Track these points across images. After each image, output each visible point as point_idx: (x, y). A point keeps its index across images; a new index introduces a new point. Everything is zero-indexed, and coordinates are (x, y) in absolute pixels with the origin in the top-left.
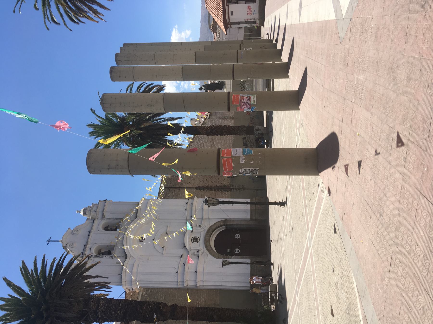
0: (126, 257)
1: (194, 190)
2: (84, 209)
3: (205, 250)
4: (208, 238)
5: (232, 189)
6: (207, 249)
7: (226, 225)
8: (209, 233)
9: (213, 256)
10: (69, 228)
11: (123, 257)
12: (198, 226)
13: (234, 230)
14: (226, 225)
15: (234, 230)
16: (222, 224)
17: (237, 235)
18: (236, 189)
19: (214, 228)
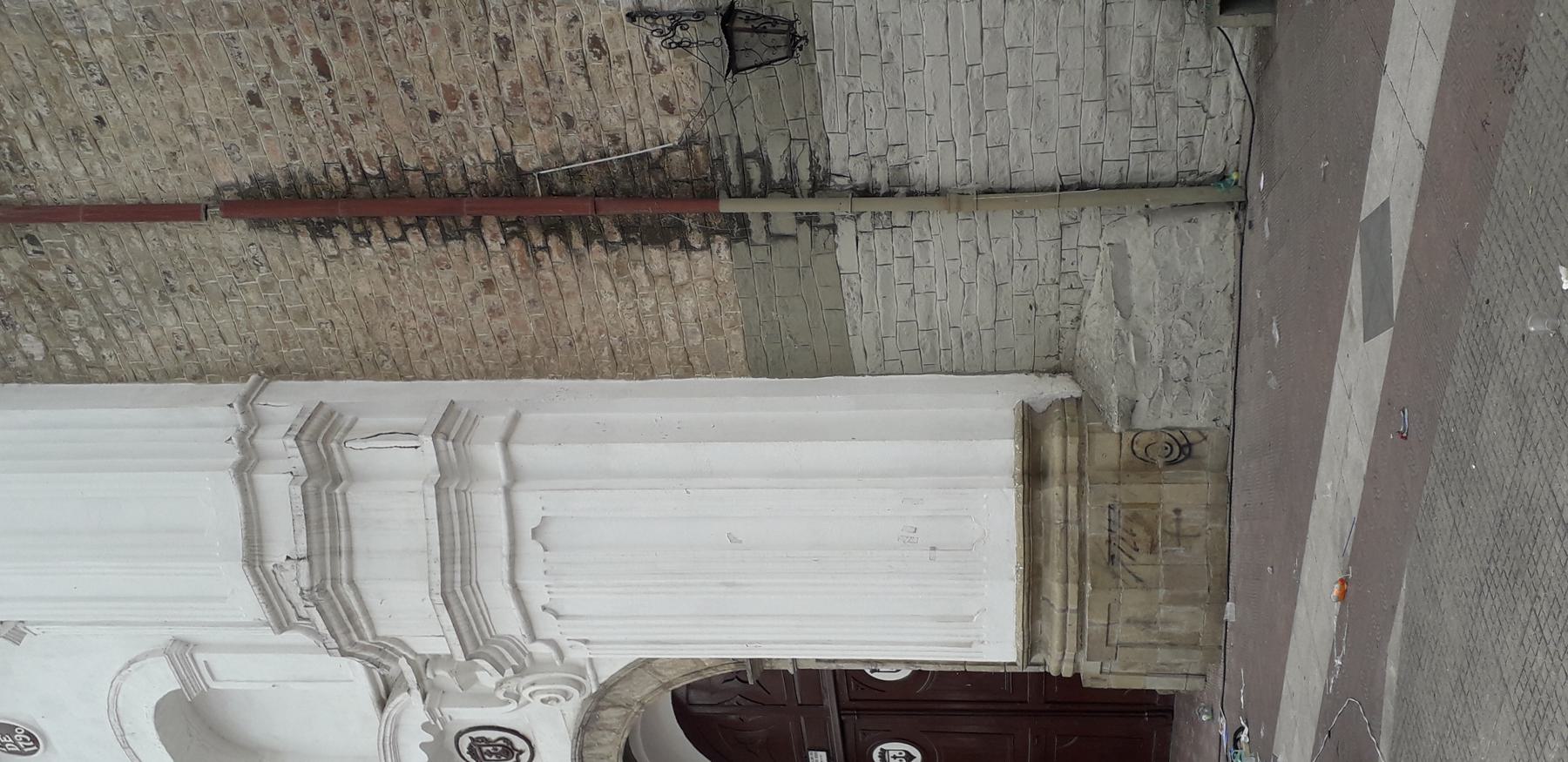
1: (233, 236)
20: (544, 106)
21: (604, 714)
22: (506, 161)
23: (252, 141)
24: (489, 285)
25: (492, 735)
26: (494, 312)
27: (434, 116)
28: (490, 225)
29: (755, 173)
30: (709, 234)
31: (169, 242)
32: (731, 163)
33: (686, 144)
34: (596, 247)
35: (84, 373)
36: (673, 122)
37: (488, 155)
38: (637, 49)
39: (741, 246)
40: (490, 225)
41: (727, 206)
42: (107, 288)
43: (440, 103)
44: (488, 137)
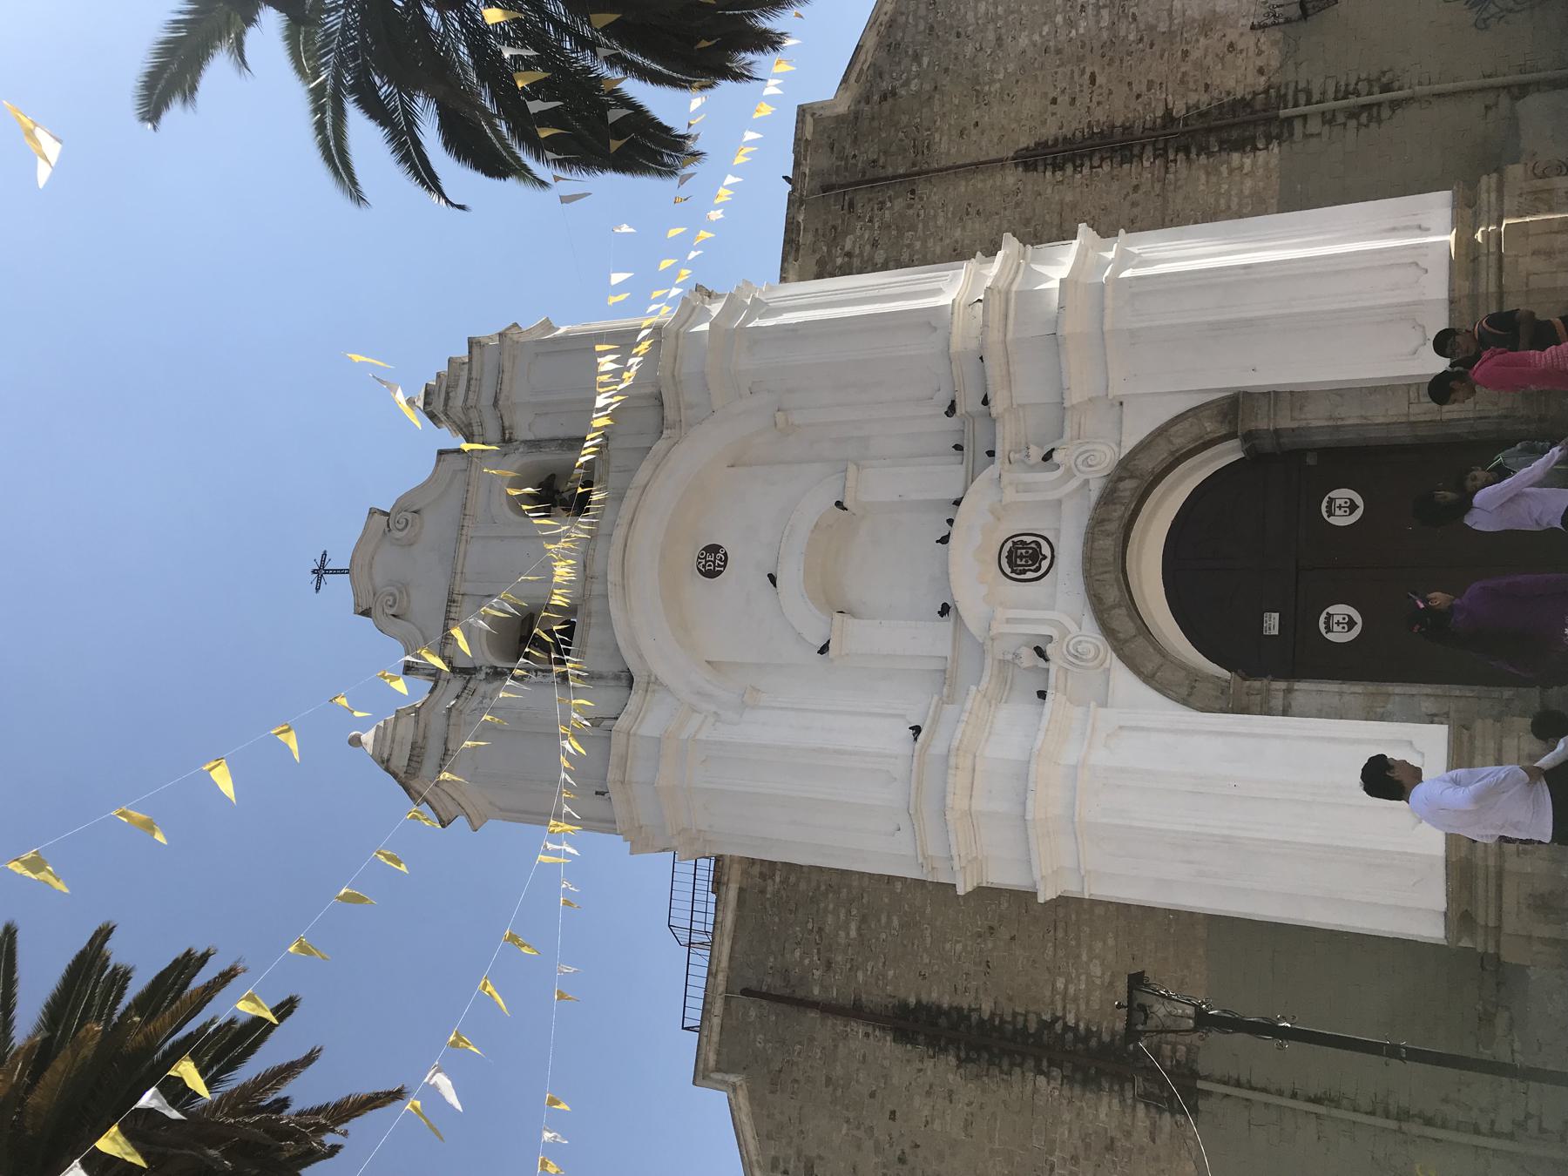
0: (631, 680)
1: (1011, 178)
2: (427, 394)
3: (1089, 636)
4: (1107, 544)
5: (1289, 120)
6: (1108, 631)
7: (1249, 437)
8: (1118, 512)
9: (1149, 679)
10: (372, 512)
11: (617, 677)
12: (1036, 454)
13: (1311, 460)
14: (1249, 437)
15: (1311, 460)
16: (1209, 426)
17: (1342, 495)
18: (1328, 119)
19: (1148, 464)
20: (1196, 82)
21: (1122, 485)
22: (1168, 112)
23: (1044, 123)
24: (1136, 188)
25: (1028, 539)
26: (1134, 204)
27: (1138, 96)
28: (1149, 149)
29: (1302, 98)
30: (1269, 139)
31: (980, 185)
32: (1290, 97)
33: (1266, 92)
34: (1203, 157)
35: (899, 265)
36: (1263, 79)
37: (1159, 113)
38: (1252, 49)
39: (1284, 145)
40: (1149, 149)
41: (1283, 113)
42: (935, 216)
43: (1144, 88)
44: (1161, 106)
